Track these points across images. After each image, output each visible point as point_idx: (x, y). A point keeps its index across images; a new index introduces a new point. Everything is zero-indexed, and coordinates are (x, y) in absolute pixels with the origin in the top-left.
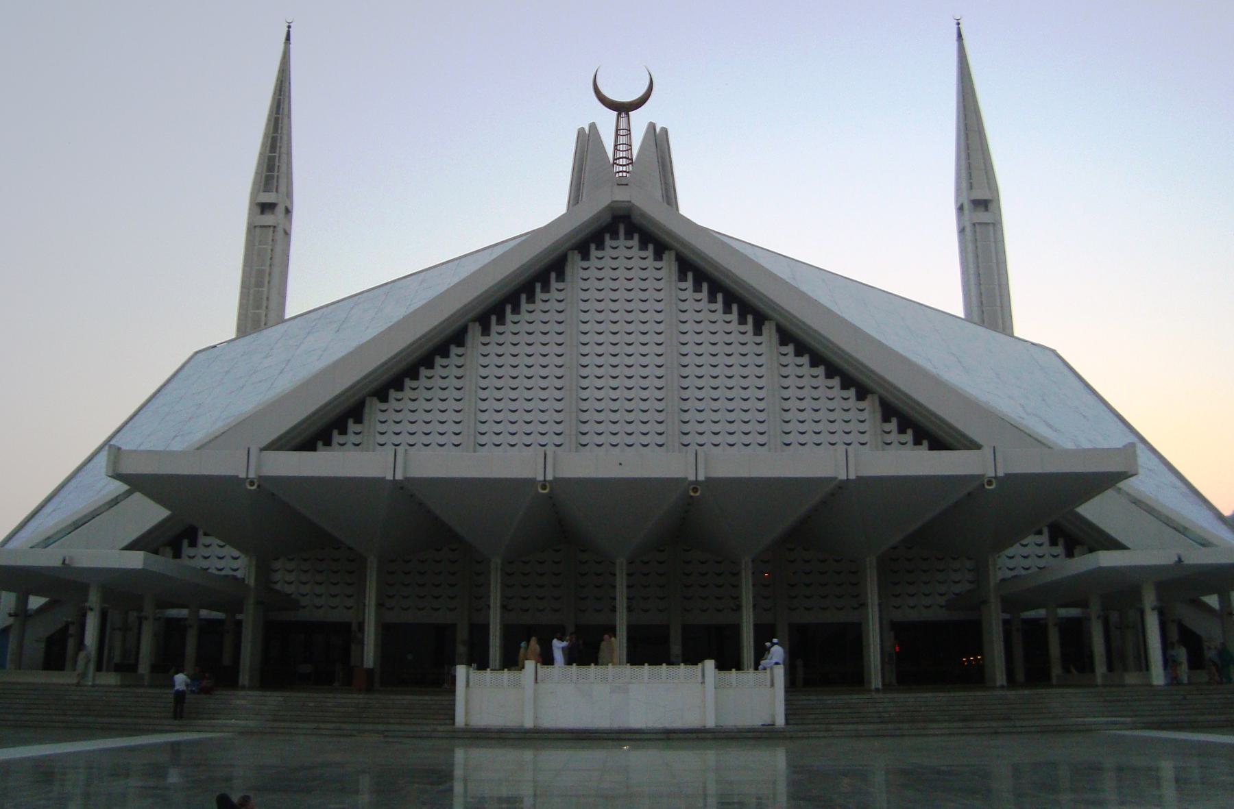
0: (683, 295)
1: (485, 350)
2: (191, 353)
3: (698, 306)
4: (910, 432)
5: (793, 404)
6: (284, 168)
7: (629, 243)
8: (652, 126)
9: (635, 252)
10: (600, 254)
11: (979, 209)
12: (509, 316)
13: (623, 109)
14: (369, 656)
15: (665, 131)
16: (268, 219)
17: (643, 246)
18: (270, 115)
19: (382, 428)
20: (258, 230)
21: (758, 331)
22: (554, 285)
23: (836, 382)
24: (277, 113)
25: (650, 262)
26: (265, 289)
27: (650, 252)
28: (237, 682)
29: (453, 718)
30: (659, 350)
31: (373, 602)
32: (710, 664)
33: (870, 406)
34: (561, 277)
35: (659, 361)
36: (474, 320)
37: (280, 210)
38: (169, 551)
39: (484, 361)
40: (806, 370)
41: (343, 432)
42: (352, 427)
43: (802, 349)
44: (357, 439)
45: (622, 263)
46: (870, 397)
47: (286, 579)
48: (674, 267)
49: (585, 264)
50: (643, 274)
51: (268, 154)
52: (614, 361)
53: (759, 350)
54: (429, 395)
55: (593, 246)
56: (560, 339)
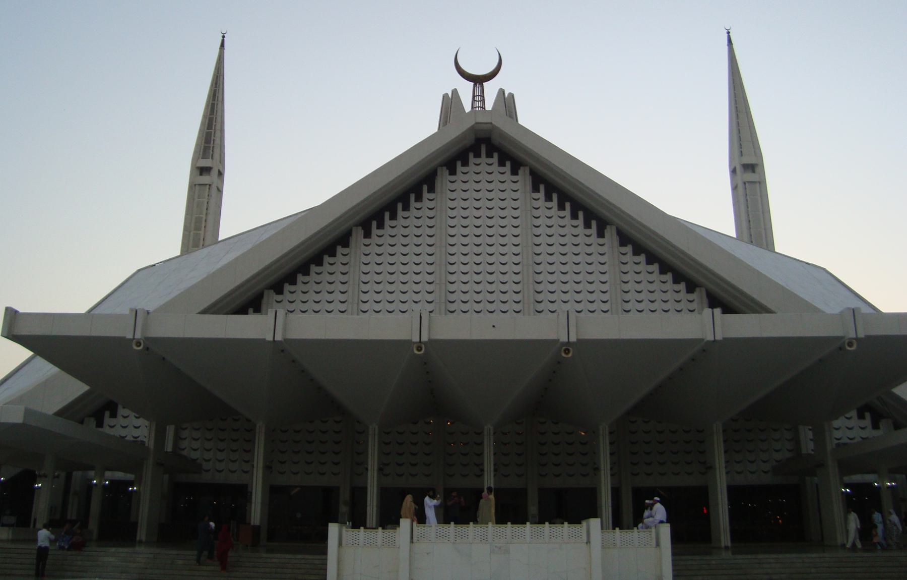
0: (536, 204)
2: (135, 270)
6: (217, 141)
7: (490, 161)
8: (502, 91)
9: (495, 168)
10: (465, 169)
11: (747, 171)
12: (388, 222)
13: (478, 81)
14: (256, 513)
15: (512, 96)
16: (205, 179)
17: (502, 164)
18: (208, 102)
20: (197, 187)
21: (601, 234)
22: (426, 195)
23: (669, 277)
24: (214, 100)
25: (508, 176)
26: (202, 232)
27: (507, 168)
28: (135, 536)
30: (516, 250)
31: (261, 464)
34: (431, 190)
35: (517, 259)
36: (357, 226)
37: (214, 173)
38: (92, 423)
39: (365, 259)
40: (643, 267)
43: (638, 249)
45: (484, 177)
46: (698, 289)
47: (194, 447)
48: (529, 180)
49: (452, 178)
51: (206, 130)
52: (478, 259)
55: (459, 163)
56: (430, 241)
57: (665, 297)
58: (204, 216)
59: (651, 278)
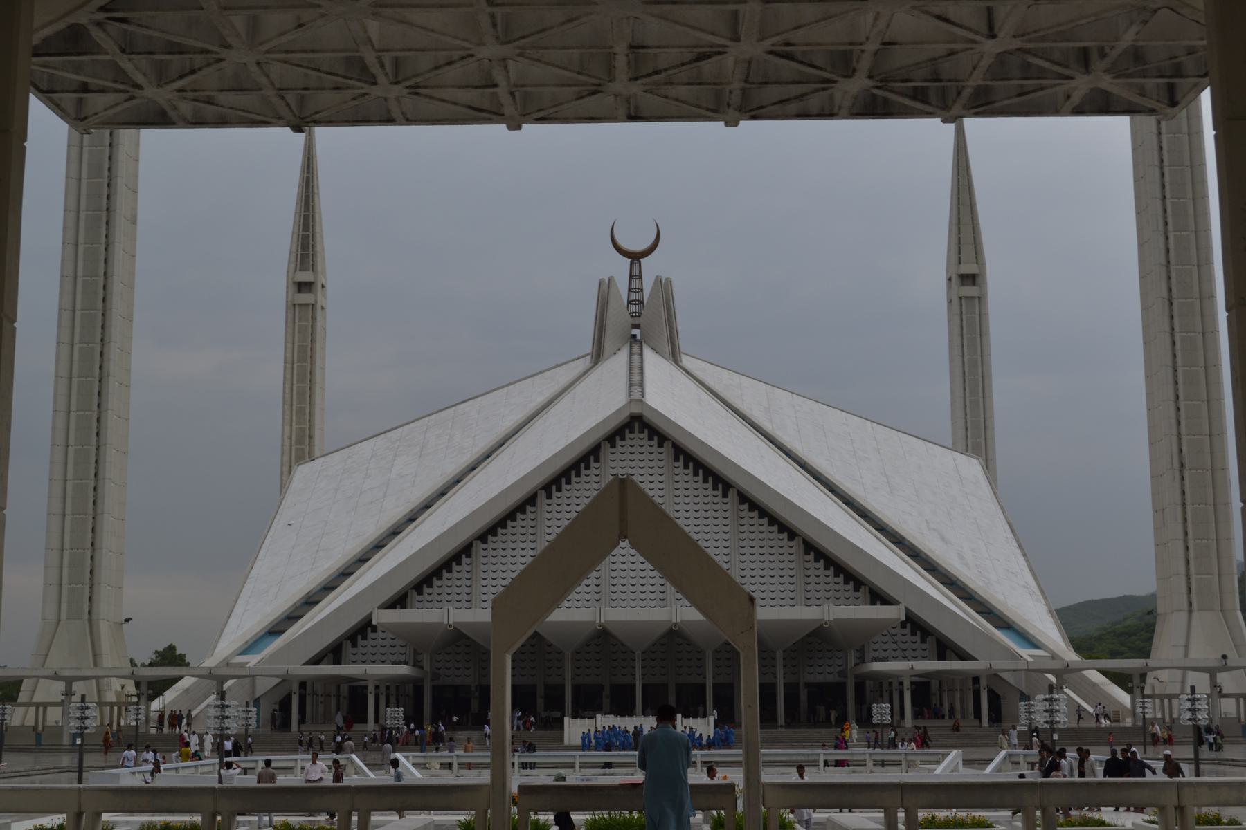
0: (677, 471)
1: (549, 508)
3: (686, 478)
6: (318, 248)
7: (642, 436)
8: (658, 280)
9: (645, 442)
10: (623, 443)
13: (635, 257)
15: (669, 283)
17: (651, 438)
19: (485, 560)
21: (725, 495)
22: (593, 464)
23: (775, 528)
24: (307, 191)
25: (655, 449)
29: (562, 741)
34: (597, 460)
40: (756, 520)
41: (459, 563)
42: (465, 560)
44: (468, 568)
45: (637, 449)
48: (672, 450)
49: (613, 450)
53: (725, 507)
54: (514, 538)
57: (772, 544)
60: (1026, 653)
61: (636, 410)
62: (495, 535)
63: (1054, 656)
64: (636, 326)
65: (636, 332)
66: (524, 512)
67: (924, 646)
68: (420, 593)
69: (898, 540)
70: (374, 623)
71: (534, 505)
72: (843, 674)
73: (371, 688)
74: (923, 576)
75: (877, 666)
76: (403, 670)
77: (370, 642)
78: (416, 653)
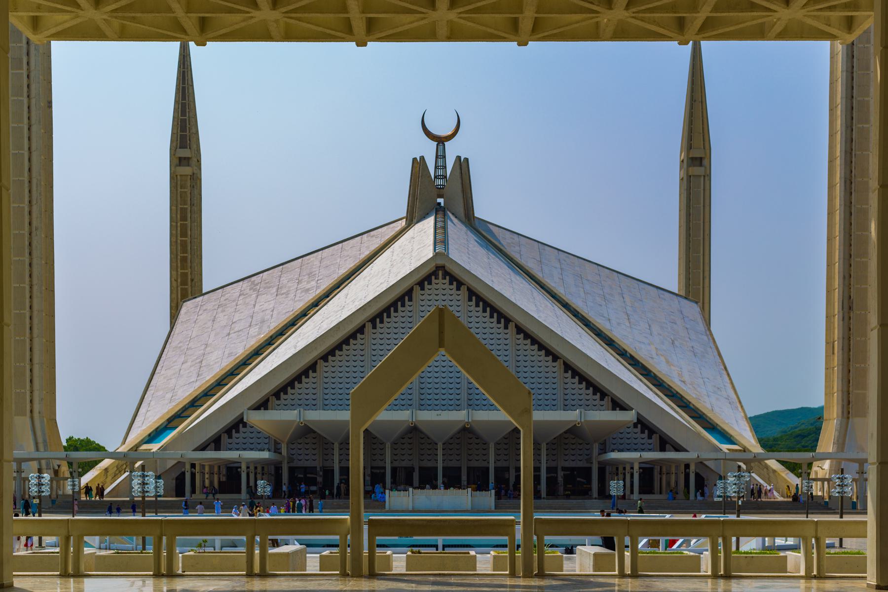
1: (374, 336)
4: (577, 377)
5: (522, 364)
7: (444, 281)
9: (447, 286)
10: (429, 287)
16: (186, 170)
17: (451, 283)
21: (506, 327)
22: (407, 303)
25: (454, 291)
26: (188, 222)
32: (470, 489)
33: (559, 363)
34: (410, 300)
40: (529, 347)
41: (307, 377)
44: (314, 380)
48: (467, 293)
49: (422, 292)
50: (451, 298)
55: (426, 283)
58: (188, 206)
59: (533, 353)
60: (725, 447)
61: (440, 262)
62: (334, 355)
63: (745, 450)
64: (440, 196)
65: (441, 201)
66: (355, 338)
67: (650, 441)
68: (278, 398)
69: (634, 363)
70: (245, 420)
71: (363, 333)
72: (589, 461)
73: (244, 467)
74: (651, 390)
75: (614, 455)
76: (265, 455)
77: (241, 435)
78: (276, 443)
